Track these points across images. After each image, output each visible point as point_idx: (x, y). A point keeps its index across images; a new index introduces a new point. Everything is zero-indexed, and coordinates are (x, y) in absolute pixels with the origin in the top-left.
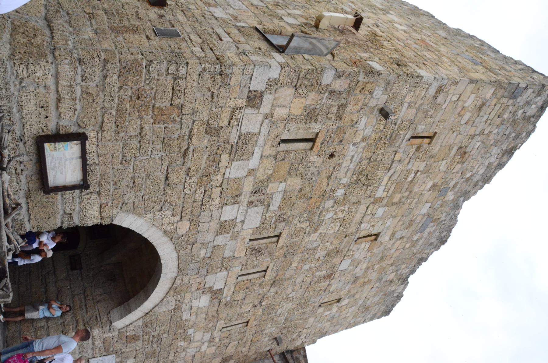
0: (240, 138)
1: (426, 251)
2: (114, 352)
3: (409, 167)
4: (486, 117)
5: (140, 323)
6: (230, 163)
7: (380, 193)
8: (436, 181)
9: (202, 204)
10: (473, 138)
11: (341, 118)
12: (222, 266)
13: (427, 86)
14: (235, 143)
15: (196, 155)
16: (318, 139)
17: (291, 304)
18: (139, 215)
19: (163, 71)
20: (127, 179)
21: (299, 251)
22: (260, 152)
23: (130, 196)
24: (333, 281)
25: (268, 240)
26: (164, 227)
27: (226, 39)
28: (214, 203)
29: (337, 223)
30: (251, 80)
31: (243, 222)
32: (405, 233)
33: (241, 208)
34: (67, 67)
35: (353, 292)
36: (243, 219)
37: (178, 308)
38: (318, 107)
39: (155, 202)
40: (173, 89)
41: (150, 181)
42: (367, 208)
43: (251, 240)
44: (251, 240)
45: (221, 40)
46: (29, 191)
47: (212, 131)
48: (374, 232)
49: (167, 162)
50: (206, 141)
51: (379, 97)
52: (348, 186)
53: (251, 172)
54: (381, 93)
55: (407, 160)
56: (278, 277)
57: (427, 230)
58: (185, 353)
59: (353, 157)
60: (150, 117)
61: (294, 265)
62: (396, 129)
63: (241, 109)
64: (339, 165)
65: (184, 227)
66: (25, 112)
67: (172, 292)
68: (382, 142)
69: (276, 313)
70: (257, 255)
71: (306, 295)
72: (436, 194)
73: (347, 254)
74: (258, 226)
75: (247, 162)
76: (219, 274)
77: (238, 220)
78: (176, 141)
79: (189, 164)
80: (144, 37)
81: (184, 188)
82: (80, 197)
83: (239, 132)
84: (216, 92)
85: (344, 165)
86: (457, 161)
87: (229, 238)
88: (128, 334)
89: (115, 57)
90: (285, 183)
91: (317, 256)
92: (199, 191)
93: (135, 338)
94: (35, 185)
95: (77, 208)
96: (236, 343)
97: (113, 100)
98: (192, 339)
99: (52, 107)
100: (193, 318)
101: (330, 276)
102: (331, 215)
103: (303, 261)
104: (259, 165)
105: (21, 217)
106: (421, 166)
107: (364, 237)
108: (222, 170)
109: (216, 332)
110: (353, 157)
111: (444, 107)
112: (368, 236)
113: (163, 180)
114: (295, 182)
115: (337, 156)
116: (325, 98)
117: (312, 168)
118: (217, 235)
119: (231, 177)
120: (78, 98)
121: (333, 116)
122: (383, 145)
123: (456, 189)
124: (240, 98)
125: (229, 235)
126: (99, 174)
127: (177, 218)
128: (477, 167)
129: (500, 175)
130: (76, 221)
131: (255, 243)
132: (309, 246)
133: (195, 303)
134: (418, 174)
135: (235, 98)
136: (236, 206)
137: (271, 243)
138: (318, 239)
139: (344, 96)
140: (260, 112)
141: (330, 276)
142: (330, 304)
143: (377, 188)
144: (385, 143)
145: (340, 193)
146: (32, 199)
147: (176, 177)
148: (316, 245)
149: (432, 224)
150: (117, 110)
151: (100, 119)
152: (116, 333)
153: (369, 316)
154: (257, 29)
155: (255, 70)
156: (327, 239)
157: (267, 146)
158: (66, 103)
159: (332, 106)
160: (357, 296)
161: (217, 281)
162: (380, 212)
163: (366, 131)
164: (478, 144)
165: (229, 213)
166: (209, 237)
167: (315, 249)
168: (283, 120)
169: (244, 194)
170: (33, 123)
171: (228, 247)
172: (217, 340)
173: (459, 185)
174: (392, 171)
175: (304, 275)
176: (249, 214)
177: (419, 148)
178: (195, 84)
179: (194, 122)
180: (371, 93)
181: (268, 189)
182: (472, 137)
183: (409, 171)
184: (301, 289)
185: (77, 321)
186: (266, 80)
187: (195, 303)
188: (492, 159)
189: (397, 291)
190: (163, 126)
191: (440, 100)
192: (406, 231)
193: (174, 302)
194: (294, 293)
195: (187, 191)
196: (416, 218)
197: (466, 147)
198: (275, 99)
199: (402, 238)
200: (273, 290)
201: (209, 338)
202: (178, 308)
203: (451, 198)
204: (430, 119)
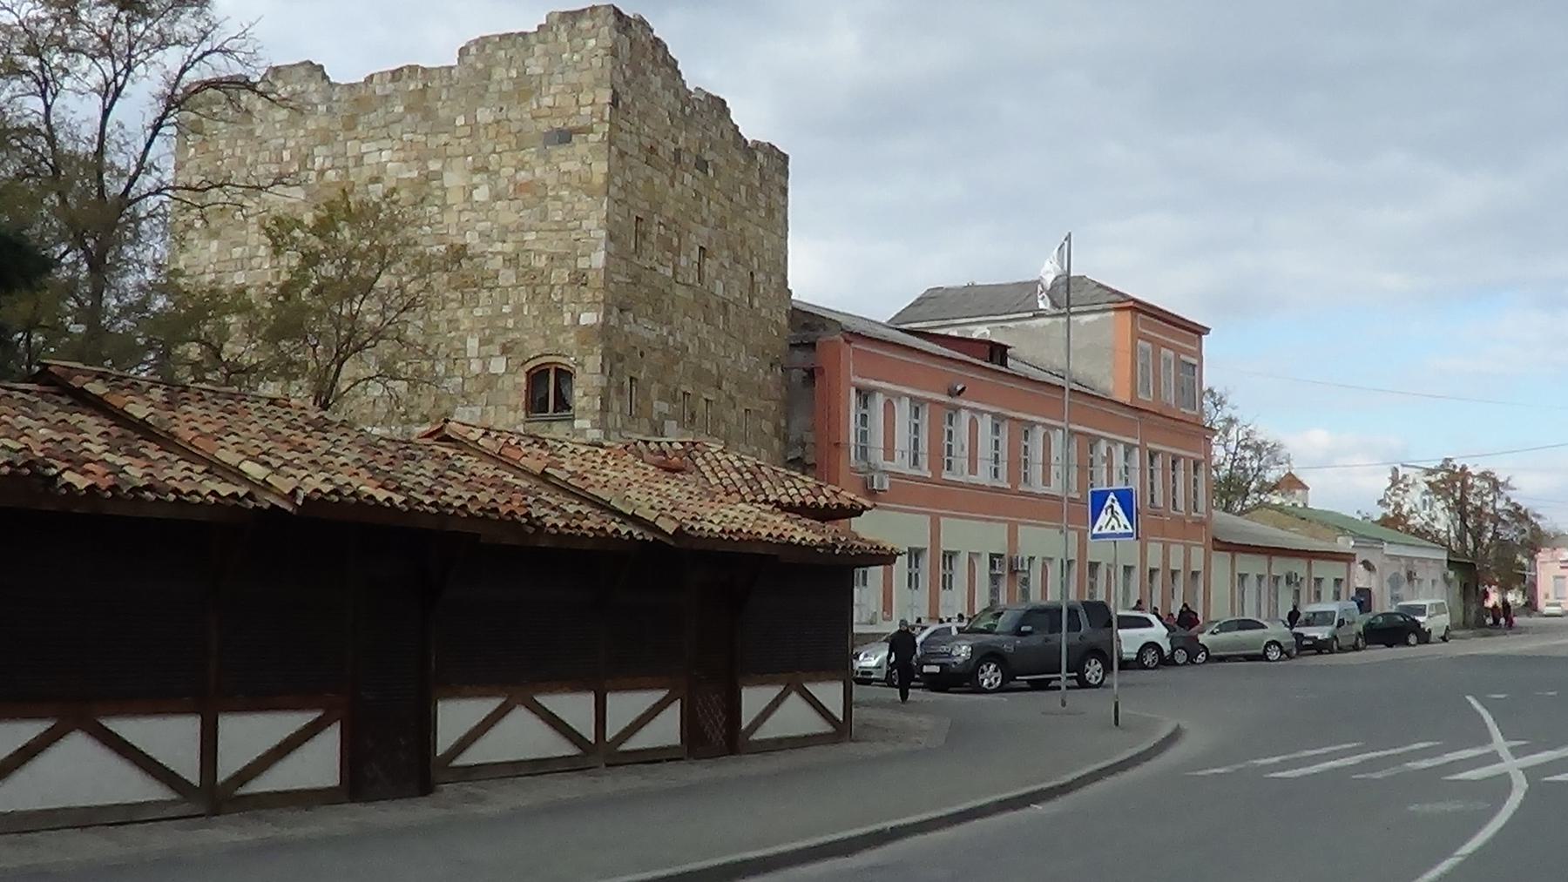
3: (654, 239)
7: (669, 273)
174: (656, 265)
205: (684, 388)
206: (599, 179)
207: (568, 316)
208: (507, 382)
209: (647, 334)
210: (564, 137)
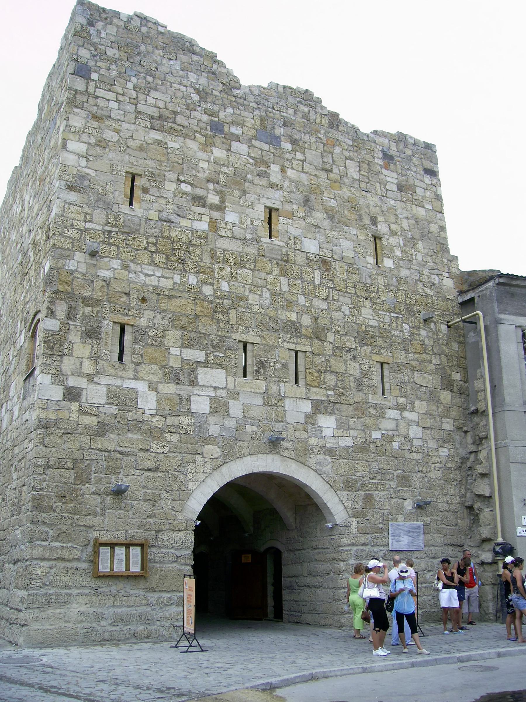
1: (318, 120)
2: (385, 522)
3: (170, 195)
5: (344, 494)
6: (139, 410)
7: (203, 226)
9: (186, 434)
10: (140, 113)
11: (99, 300)
12: (275, 405)
13: (67, 206)
14: (116, 407)
15: (126, 444)
16: (121, 322)
17: (363, 310)
19: (41, 478)
20: (145, 506)
21: (272, 314)
23: (166, 503)
24: (335, 257)
26: (208, 471)
28: (185, 423)
30: (52, 401)
31: (215, 388)
32: (275, 168)
34: (34, 551)
36: (212, 389)
37: (330, 452)
38: (84, 329)
39: (176, 481)
40: (58, 468)
41: (150, 485)
42: (223, 236)
43: (245, 376)
45: (27, 420)
46: (147, 588)
47: (102, 430)
49: (132, 470)
50: (112, 436)
51: (78, 262)
52: (184, 272)
54: (72, 261)
55: (163, 201)
56: (309, 334)
57: (279, 131)
59: (146, 275)
60: (83, 487)
61: (293, 317)
62: (117, 230)
63: (81, 406)
64: (155, 288)
66: (70, 584)
67: (301, 460)
68: (131, 242)
69: (374, 327)
70: (268, 366)
73: (293, 246)
75: (140, 393)
76: (286, 408)
77: (212, 394)
78: (110, 464)
79: (135, 450)
81: (163, 453)
82: (160, 547)
83: (105, 406)
84: (62, 431)
85: (156, 283)
86: (170, 124)
87: (235, 402)
89: (29, 515)
90: (171, 349)
91: (285, 288)
92: (168, 439)
94: (142, 584)
95: (172, 551)
96: (416, 374)
97: (65, 518)
98: (391, 432)
99: (69, 565)
100: (353, 433)
104: (145, 380)
105: (176, 598)
108: (146, 417)
109: (387, 403)
112: (270, 223)
113: (150, 474)
115: (142, 294)
116: (75, 323)
118: (228, 415)
119: (155, 408)
120: (61, 544)
121: (96, 310)
122: (136, 239)
123: (216, 108)
124: (70, 408)
125: (231, 402)
126: (137, 530)
127: (199, 458)
128: (183, 89)
130: (188, 552)
131: (249, 370)
134: (182, 178)
135: (70, 413)
136: (192, 398)
140: (85, 387)
141: (325, 264)
143: (193, 231)
144: (134, 238)
145: (193, 280)
146: (155, 587)
147: (149, 462)
148: (268, 293)
150: (75, 514)
151: (82, 528)
152: (353, 520)
154: (25, 380)
155: (43, 398)
156: (260, 282)
157: (123, 375)
158: (66, 554)
159: (84, 313)
161: (297, 409)
162: (231, 217)
163: (116, 267)
165: (201, 404)
167: (273, 293)
168: (96, 363)
169: (178, 392)
170: (81, 579)
171: (248, 401)
172: (402, 400)
173: (210, 106)
174: (173, 218)
175: (315, 300)
176: (205, 384)
177: (145, 190)
178: (54, 450)
180: (72, 272)
183: (178, 193)
184: (338, 300)
185: (333, 559)
186: (54, 386)
187: (328, 432)
188: (176, 66)
190: (94, 475)
193: (318, 457)
194: (343, 308)
195: (166, 450)
196: (253, 158)
197: (152, 118)
198: (73, 375)
201: (396, 411)
202: (330, 452)
203: (230, 110)
204: (108, 188)
209: (154, 281)
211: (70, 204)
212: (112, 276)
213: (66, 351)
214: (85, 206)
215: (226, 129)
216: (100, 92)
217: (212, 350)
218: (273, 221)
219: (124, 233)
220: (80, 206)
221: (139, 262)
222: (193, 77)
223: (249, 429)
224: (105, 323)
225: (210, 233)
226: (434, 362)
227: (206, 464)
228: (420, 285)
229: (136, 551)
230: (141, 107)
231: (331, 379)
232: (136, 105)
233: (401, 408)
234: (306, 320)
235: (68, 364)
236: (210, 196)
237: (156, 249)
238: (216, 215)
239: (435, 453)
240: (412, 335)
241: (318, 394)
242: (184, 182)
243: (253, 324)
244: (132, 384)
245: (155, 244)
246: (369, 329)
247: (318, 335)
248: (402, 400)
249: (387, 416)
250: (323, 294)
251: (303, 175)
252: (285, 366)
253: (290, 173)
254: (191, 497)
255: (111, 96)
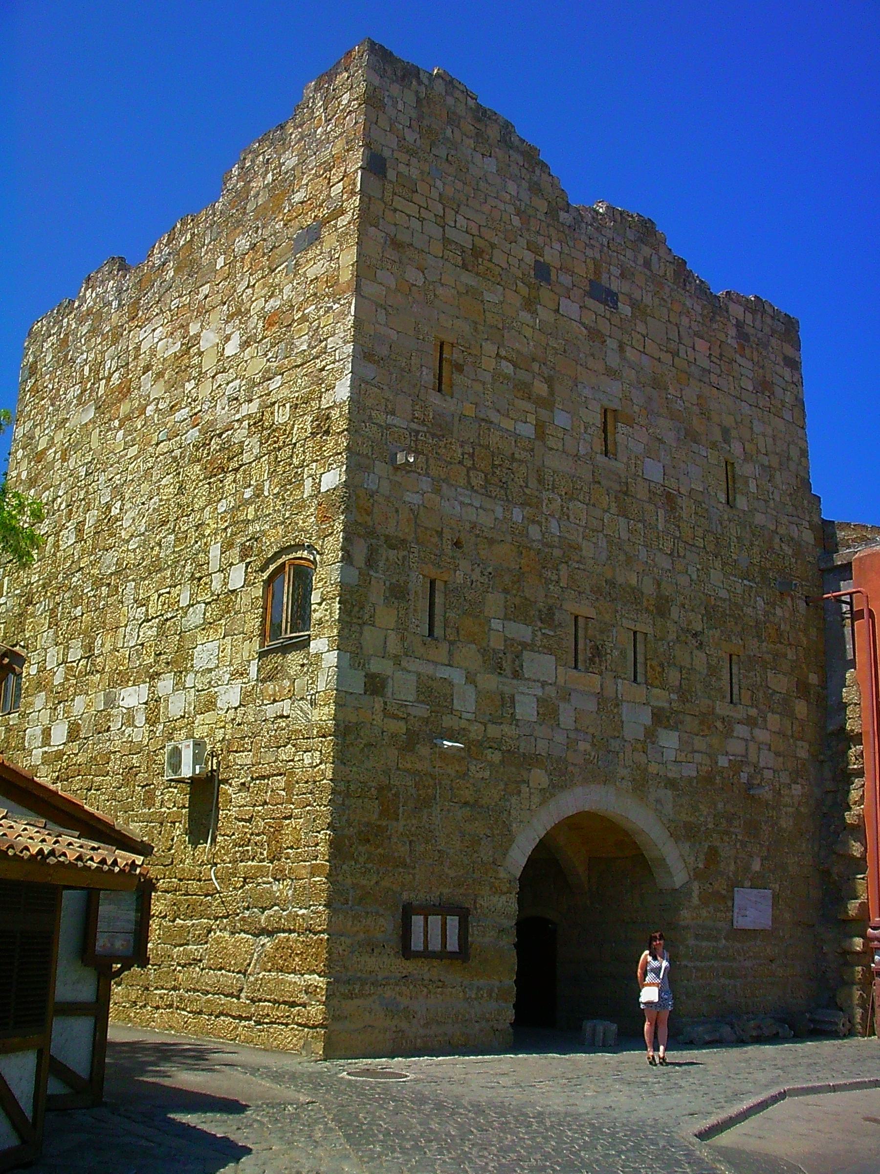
0: (422, 702)
3: (488, 377)
4: (415, 224)
7: (527, 430)
8: (517, 302)
18: (512, 841)
22: (445, 668)
24: (682, 490)
25: (581, 633)
27: (285, 707)
29: (571, 506)
31: (544, 684)
32: (612, 344)
33: (521, 689)
35: (717, 436)
37: (671, 784)
44: (576, 667)
48: (598, 420)
53: (470, 679)
58: (766, 772)
59: (462, 503)
62: (425, 429)
65: (539, 777)
69: (725, 600)
71: (700, 543)
72: (545, 294)
74: (554, 658)
80: (287, 822)
83: (415, 704)
85: (473, 518)
88: (701, 866)
91: (625, 536)
93: (712, 855)
98: (739, 758)
100: (698, 757)
101: (670, 500)
102: (554, 525)
103: (630, 560)
106: (490, 348)
107: (606, 440)
108: (463, 724)
110: (462, 503)
111: (394, 336)
112: (605, 431)
114: (494, 603)
117: (474, 578)
123: (540, 240)
125: (562, 706)
128: (502, 206)
129: (525, 130)
130: (510, 923)
132: (604, 556)
133: (670, 755)
134: (503, 353)
136: (517, 698)
137: (586, 629)
138: (594, 540)
139: (374, 541)
142: (734, 483)
145: (517, 514)
147: (467, 791)
149: (605, 276)
153: (788, 378)
159: (387, 559)
160: (728, 421)
161: (636, 720)
162: (562, 419)
164: (461, 222)
165: (526, 709)
166: (560, 738)
167: (610, 542)
168: (403, 639)
172: (753, 712)
175: (659, 554)
177: (459, 368)
178: (355, 769)
179: (398, 769)
181: (498, 648)
182: (446, 241)
184: (684, 557)
187: (670, 755)
188: (491, 165)
189: (741, 318)
191: (384, 351)
192: (609, 340)
194: (692, 570)
199: (621, 348)
200: (674, 615)
202: (671, 784)
205: (571, 607)
206: (346, 275)
207: (308, 483)
208: (242, 602)
209: (471, 514)
210: (312, 236)
211: (367, 383)
212: (421, 502)
213: (366, 617)
214: (385, 387)
215: (553, 277)
216: (399, 203)
217: (539, 624)
218: (610, 428)
219: (434, 436)
220: (379, 388)
221: (454, 482)
222: (512, 187)
223: (583, 746)
224: (413, 575)
225: (537, 443)
226: (789, 657)
227: (532, 796)
228: (777, 540)
229: (453, 922)
230: (451, 234)
231: (674, 677)
232: (443, 227)
233: (751, 722)
234: (648, 588)
235: (370, 637)
236: (536, 383)
237: (473, 464)
238: (544, 414)
239: (787, 792)
240: (766, 614)
241: (661, 698)
242: (505, 358)
243: (588, 589)
244: (444, 672)
245: (472, 456)
246: (719, 603)
247: (662, 608)
248: (753, 712)
249: (735, 734)
250: (668, 546)
251: (644, 357)
252: (623, 653)
253: (630, 353)
254: (514, 845)
255: (412, 209)
